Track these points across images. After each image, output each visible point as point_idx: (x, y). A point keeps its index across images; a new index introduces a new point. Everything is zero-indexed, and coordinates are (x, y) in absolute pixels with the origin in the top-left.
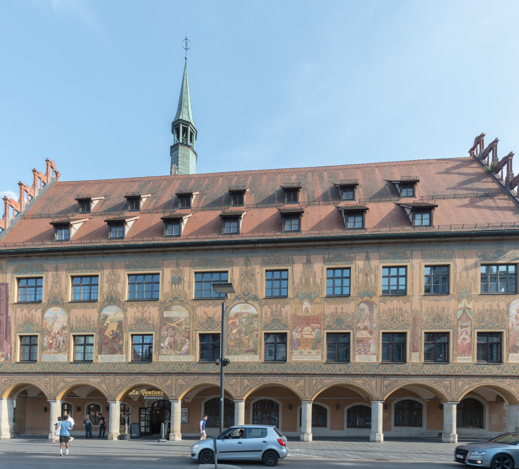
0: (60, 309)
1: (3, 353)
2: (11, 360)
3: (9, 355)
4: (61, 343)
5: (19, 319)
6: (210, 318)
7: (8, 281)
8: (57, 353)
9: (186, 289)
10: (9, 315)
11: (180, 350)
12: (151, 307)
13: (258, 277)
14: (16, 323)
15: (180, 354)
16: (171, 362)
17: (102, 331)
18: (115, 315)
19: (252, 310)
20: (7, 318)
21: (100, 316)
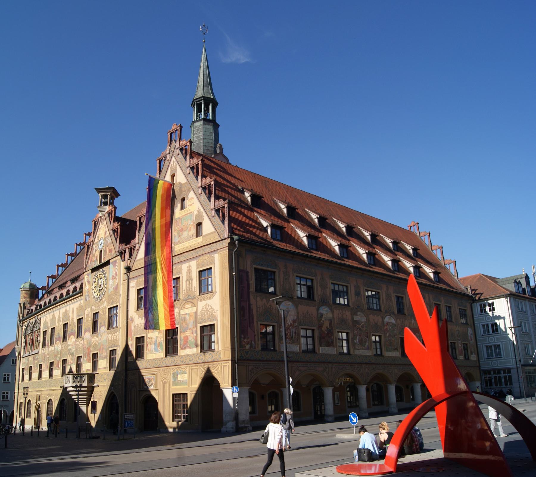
0: (291, 303)
1: (249, 340)
2: (255, 348)
3: (253, 342)
4: (294, 334)
5: (260, 308)
6: (376, 324)
7: (248, 269)
8: (291, 344)
9: (363, 301)
10: (251, 302)
11: (364, 346)
12: (347, 311)
13: (393, 298)
14: (257, 311)
15: (365, 349)
16: (361, 355)
17: (320, 326)
18: (327, 314)
19: (393, 321)
20: (250, 305)
21: (318, 314)
